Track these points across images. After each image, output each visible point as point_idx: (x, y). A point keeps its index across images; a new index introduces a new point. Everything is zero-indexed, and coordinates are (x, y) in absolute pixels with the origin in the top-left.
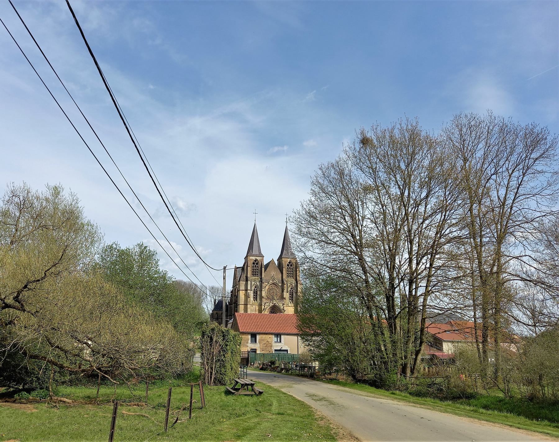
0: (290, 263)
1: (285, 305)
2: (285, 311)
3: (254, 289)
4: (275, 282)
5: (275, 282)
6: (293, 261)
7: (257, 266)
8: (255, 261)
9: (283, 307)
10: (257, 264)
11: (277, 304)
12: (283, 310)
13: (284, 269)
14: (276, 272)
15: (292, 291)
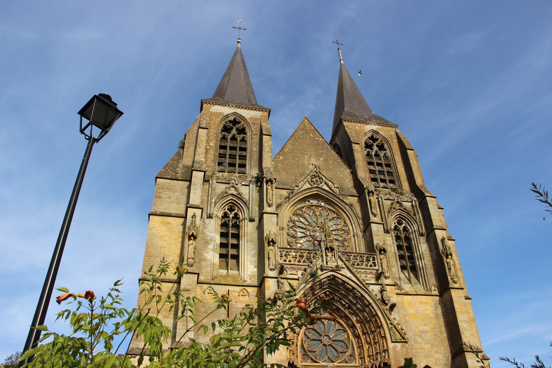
0: (372, 138)
1: (388, 281)
2: (393, 306)
3: (225, 215)
4: (325, 187)
5: (325, 187)
6: (385, 132)
7: (239, 137)
8: (234, 122)
9: (376, 289)
10: (242, 131)
11: (345, 272)
12: (383, 301)
13: (355, 147)
14: (326, 160)
15: (405, 229)
